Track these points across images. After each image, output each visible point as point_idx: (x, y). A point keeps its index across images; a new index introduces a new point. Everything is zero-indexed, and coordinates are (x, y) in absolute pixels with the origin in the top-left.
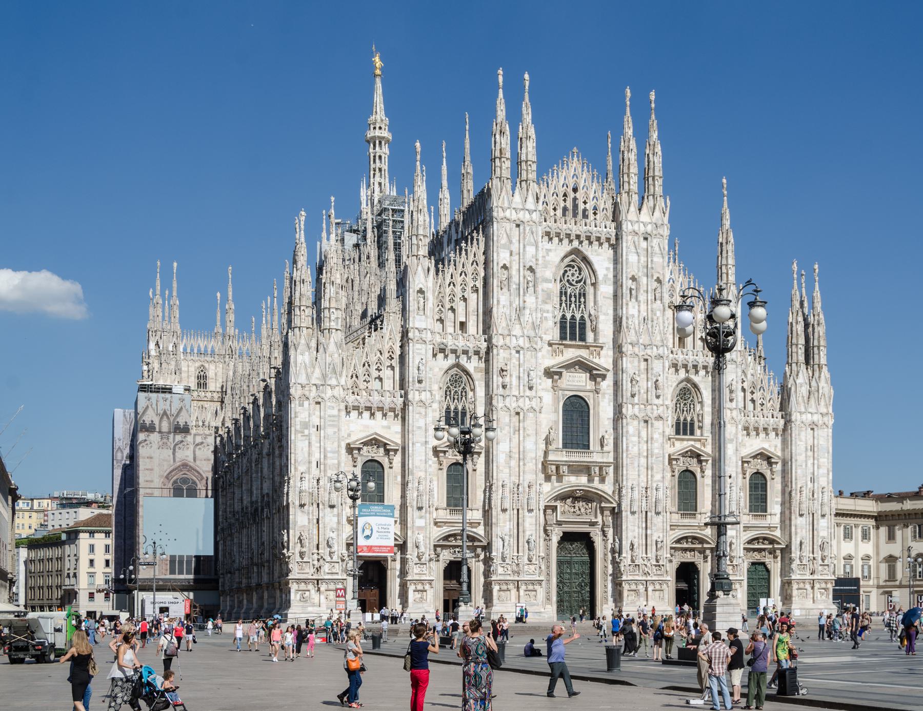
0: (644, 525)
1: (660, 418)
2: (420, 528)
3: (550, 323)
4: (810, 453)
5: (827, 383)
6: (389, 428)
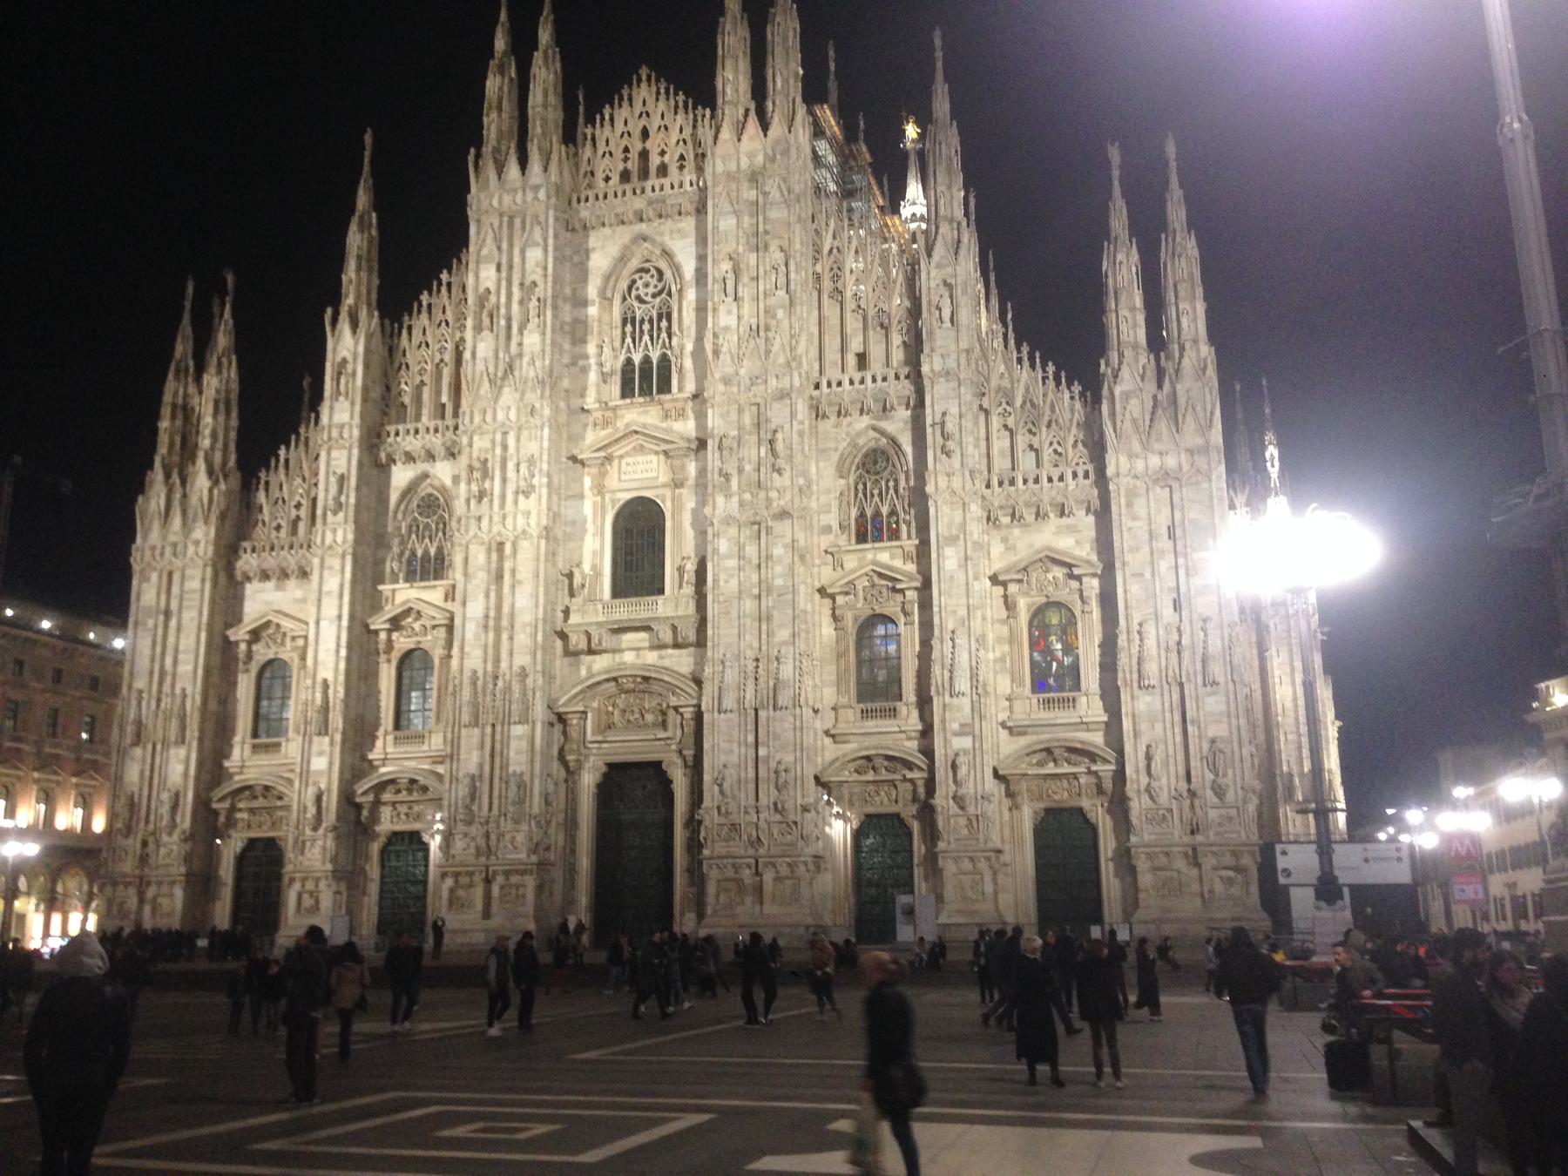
0: (751, 738)
1: (783, 515)
2: (320, 772)
3: (593, 376)
4: (1164, 544)
5: (1198, 379)
6: (304, 601)
